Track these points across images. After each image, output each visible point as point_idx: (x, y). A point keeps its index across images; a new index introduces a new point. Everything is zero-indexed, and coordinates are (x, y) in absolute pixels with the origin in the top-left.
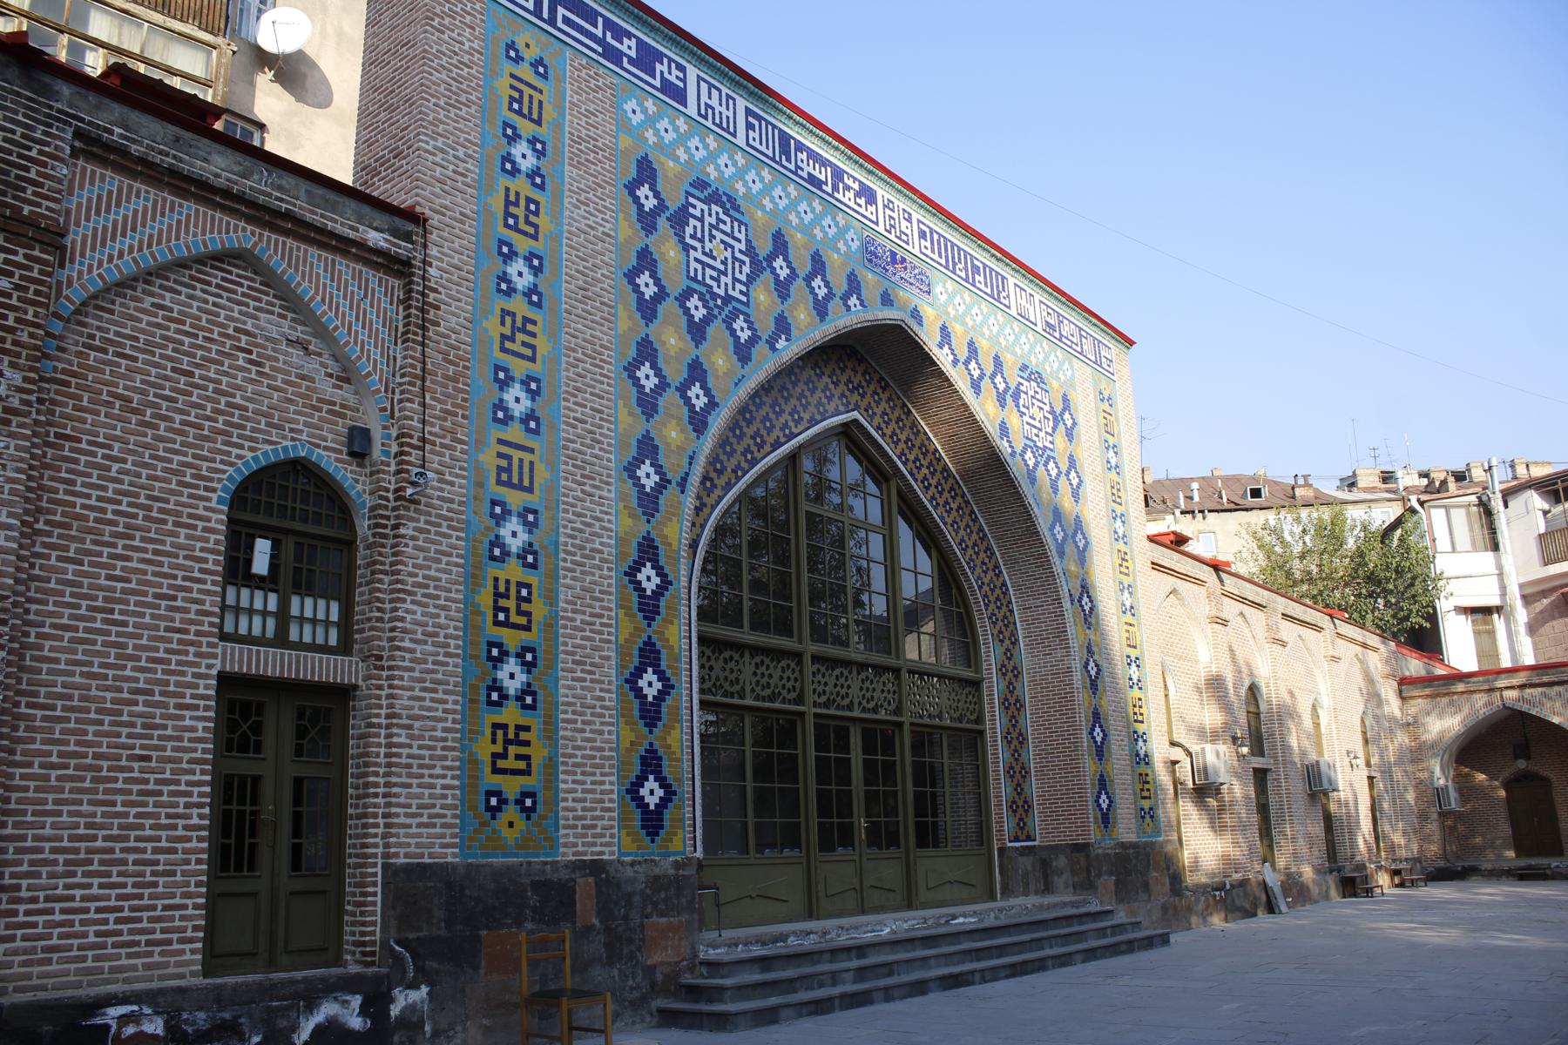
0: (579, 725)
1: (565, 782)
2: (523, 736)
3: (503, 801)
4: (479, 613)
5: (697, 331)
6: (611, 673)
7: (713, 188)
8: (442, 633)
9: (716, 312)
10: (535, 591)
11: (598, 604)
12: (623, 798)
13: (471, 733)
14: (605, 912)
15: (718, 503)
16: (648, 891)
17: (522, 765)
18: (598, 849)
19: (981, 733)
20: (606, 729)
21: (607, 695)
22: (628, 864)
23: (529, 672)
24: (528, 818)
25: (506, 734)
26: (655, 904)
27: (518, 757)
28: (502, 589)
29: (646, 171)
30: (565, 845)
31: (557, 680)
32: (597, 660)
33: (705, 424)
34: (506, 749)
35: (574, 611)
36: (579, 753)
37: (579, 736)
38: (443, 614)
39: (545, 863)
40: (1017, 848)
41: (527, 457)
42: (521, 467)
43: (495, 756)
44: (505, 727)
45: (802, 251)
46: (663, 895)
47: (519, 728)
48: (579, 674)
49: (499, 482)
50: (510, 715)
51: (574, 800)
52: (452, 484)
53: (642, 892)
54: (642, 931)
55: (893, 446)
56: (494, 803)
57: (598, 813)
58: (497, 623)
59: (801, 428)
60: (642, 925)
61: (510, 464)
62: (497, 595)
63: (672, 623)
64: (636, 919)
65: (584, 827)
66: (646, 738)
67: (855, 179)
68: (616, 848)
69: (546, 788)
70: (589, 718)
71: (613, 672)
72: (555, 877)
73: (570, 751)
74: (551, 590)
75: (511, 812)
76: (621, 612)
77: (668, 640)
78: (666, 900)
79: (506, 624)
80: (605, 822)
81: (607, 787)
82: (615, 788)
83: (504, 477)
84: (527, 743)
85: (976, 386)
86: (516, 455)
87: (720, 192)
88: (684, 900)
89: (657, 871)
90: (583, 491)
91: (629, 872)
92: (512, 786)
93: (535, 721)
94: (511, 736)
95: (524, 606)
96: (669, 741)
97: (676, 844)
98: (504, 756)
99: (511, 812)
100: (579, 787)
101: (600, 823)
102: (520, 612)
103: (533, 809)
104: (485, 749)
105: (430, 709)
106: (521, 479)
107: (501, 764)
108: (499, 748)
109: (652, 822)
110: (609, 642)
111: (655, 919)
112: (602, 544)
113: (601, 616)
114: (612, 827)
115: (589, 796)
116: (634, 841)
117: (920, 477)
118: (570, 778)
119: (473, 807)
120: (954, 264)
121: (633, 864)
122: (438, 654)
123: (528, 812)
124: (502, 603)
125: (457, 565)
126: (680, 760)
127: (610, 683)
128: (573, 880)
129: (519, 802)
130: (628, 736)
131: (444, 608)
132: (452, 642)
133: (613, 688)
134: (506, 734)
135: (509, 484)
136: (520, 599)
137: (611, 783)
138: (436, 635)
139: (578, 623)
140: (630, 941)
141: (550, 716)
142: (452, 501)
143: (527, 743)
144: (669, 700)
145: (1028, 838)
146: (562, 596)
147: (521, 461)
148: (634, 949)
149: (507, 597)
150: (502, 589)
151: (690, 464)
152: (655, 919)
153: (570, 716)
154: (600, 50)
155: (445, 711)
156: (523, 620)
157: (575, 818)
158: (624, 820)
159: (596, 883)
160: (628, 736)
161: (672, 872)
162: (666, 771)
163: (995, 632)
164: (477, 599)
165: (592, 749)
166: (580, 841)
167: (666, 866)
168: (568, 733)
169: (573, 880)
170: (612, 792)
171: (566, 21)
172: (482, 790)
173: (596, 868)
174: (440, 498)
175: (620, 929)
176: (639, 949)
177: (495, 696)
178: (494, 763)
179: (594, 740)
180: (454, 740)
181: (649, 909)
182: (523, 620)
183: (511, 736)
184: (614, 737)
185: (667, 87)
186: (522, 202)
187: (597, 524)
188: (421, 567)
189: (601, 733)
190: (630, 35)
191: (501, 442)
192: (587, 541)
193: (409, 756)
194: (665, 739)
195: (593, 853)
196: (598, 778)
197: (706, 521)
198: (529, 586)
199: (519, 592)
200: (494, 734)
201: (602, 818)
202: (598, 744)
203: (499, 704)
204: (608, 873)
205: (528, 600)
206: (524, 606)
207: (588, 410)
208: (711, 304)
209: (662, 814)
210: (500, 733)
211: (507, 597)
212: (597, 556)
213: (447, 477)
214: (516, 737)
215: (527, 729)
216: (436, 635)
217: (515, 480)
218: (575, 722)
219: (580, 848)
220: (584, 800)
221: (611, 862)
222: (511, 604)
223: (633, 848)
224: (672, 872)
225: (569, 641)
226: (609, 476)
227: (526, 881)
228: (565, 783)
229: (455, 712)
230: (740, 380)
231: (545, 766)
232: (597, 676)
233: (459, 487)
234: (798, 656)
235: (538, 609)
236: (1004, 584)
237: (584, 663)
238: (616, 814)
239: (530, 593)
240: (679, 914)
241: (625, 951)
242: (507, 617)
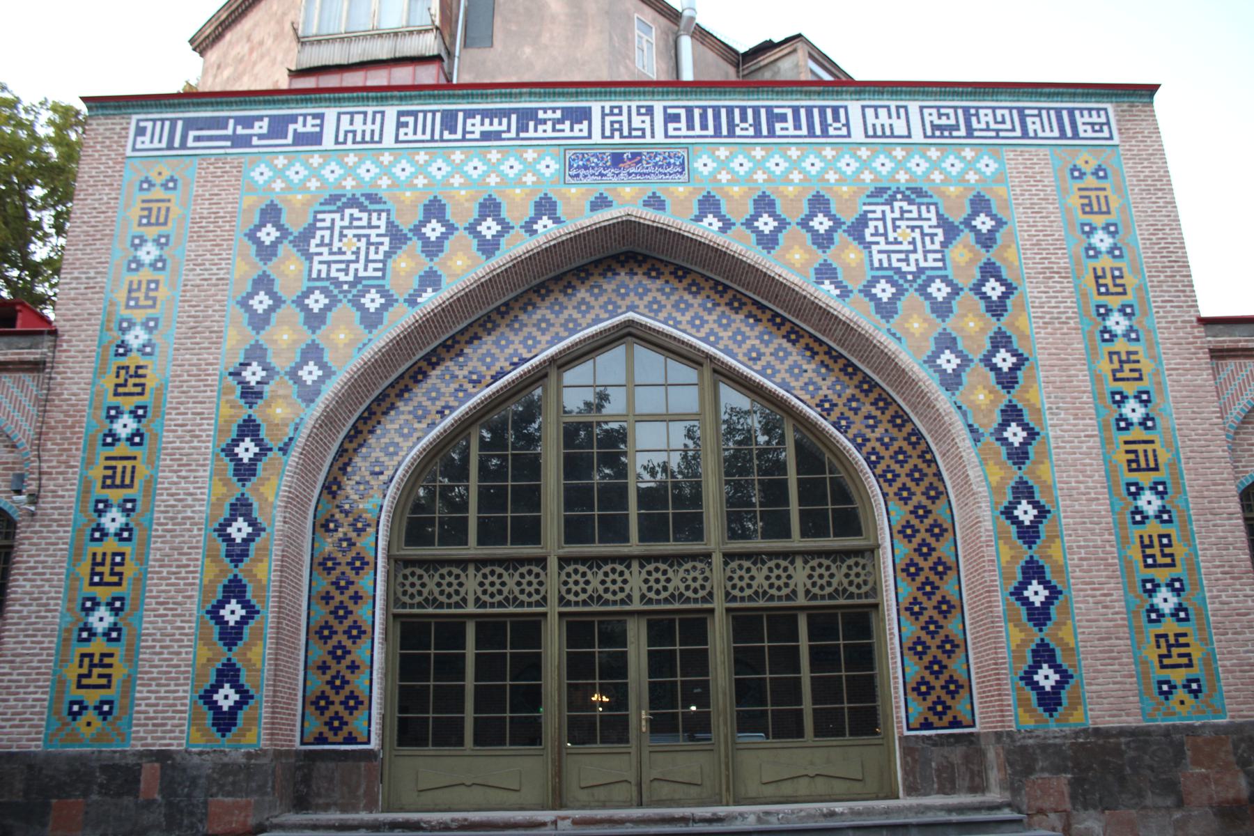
0: (158, 649)
1: (140, 692)
2: (107, 660)
3: (83, 708)
4: (78, 579)
5: (315, 320)
6: (194, 607)
7: (349, 195)
8: (45, 596)
9: (340, 296)
10: (127, 558)
11: (184, 558)
12: (196, 702)
13: (63, 661)
14: (168, 788)
15: (415, 444)
16: (215, 776)
17: (104, 681)
18: (167, 741)
19: (876, 606)
20: (183, 650)
21: (186, 625)
22: (195, 753)
23: (116, 615)
24: (105, 719)
25: (91, 661)
26: (221, 787)
27: (100, 676)
28: (99, 559)
29: (271, 213)
30: (135, 739)
31: (142, 617)
32: (180, 599)
33: (318, 393)
34: (90, 671)
35: (161, 566)
36: (155, 670)
37: (156, 657)
38: (47, 584)
39: (115, 752)
40: (929, 738)
41: (129, 464)
42: (124, 472)
43: (81, 676)
44: (91, 655)
45: (466, 205)
46: (231, 779)
47: (103, 655)
48: (162, 612)
49: (104, 486)
50: (97, 646)
51: (147, 705)
52: (63, 497)
53: (208, 777)
54: (206, 808)
55: (693, 331)
56: (76, 710)
57: (170, 714)
58: (92, 584)
59: (534, 352)
60: (206, 803)
61: (115, 473)
62: (95, 564)
63: (261, 561)
64: (199, 796)
65: (154, 725)
66: (224, 654)
67: (554, 110)
68: (184, 742)
69: (123, 697)
70: (168, 643)
71: (195, 607)
72: (123, 762)
73: (147, 669)
74: (142, 554)
75: (90, 715)
76: (207, 561)
77: (255, 576)
78: (234, 783)
79: (101, 583)
80: (176, 722)
81: (181, 694)
82: (188, 695)
83: (109, 482)
84: (110, 666)
85: (768, 241)
86: (120, 465)
87: (358, 195)
88: (254, 785)
89: (226, 760)
90: (179, 477)
91: (196, 760)
92: (92, 697)
93: (119, 650)
94: (96, 660)
95: (117, 569)
96: (249, 655)
97: (251, 738)
98: (89, 676)
99: (90, 715)
100: (153, 696)
101: (170, 722)
102: (113, 574)
103: (110, 712)
104: (72, 672)
105: (29, 648)
106: (123, 480)
107: (85, 681)
108: (85, 671)
109: (225, 721)
110: (193, 584)
111: (220, 798)
112: (193, 512)
113: (188, 566)
114: (182, 725)
115: (162, 702)
116: (202, 736)
117: (740, 352)
118: (145, 689)
119: (58, 713)
120: (731, 126)
121: (201, 753)
122: (39, 611)
123: (105, 715)
124: (98, 569)
125: (61, 550)
126: (260, 671)
127: (191, 615)
128: (140, 765)
129: (98, 708)
130: (205, 653)
131: (47, 580)
132: (52, 602)
133: (194, 619)
134: (91, 661)
135: (113, 486)
136: (114, 564)
137: (185, 691)
138: (41, 599)
139: (165, 574)
140: (192, 814)
141: (132, 645)
142: (61, 508)
143: (110, 666)
144: (252, 623)
145: (955, 723)
146: (151, 557)
147: (124, 468)
148: (194, 820)
149: (102, 564)
150: (99, 559)
151: (296, 429)
152: (220, 798)
153: (150, 643)
154: (229, 143)
155: (42, 649)
156: (116, 579)
157: (146, 719)
158: (195, 719)
159: (162, 768)
160: (205, 653)
161: (244, 760)
162: (243, 680)
163: (891, 491)
164: (77, 570)
165: (168, 666)
166: (149, 736)
167: (237, 756)
168: (146, 656)
169: (140, 765)
170: (185, 698)
171: (197, 139)
172: (68, 698)
173: (163, 756)
174: (52, 508)
175: (182, 804)
176: (201, 821)
177: (85, 635)
178: (79, 681)
179: (172, 660)
180: (47, 668)
181: (214, 790)
182: (116, 579)
183: (96, 660)
184: (191, 656)
185: (300, 139)
186: (144, 286)
187: (189, 498)
188: (32, 556)
189: (179, 653)
190: (260, 118)
191: (108, 458)
192: (179, 512)
193: (10, 681)
194: (245, 654)
195: (161, 745)
196: (172, 688)
197: (400, 464)
198: (122, 555)
199: (113, 559)
200: (81, 661)
201: (173, 718)
202: (175, 662)
203: (88, 640)
204: (173, 759)
205: (121, 564)
206: (117, 569)
207: (190, 416)
208: (336, 292)
209: (236, 714)
210: (86, 660)
211: (102, 564)
212: (188, 522)
213: (60, 493)
214: (104, 661)
215: (111, 655)
216: (41, 599)
217: (118, 481)
218: (154, 647)
219: (149, 741)
220: (157, 705)
221: (178, 752)
222: (106, 569)
223: (202, 741)
224: (244, 760)
225: (155, 587)
226: (205, 459)
227: (97, 764)
228: (141, 692)
229: (49, 648)
230: (365, 345)
231: (124, 681)
232: (179, 612)
233: (70, 496)
234: (541, 561)
235: (129, 570)
236: (916, 432)
237: (168, 603)
238: (187, 715)
239: (123, 559)
240: (247, 795)
241: (186, 822)
242: (101, 579)
